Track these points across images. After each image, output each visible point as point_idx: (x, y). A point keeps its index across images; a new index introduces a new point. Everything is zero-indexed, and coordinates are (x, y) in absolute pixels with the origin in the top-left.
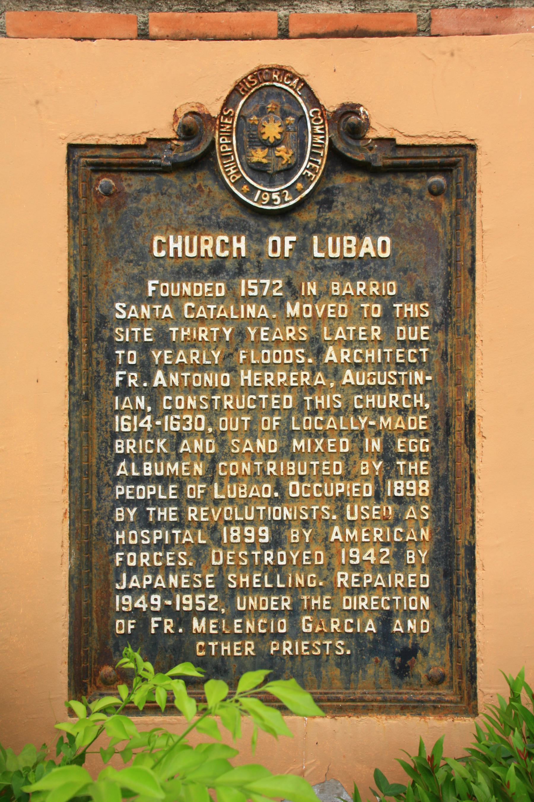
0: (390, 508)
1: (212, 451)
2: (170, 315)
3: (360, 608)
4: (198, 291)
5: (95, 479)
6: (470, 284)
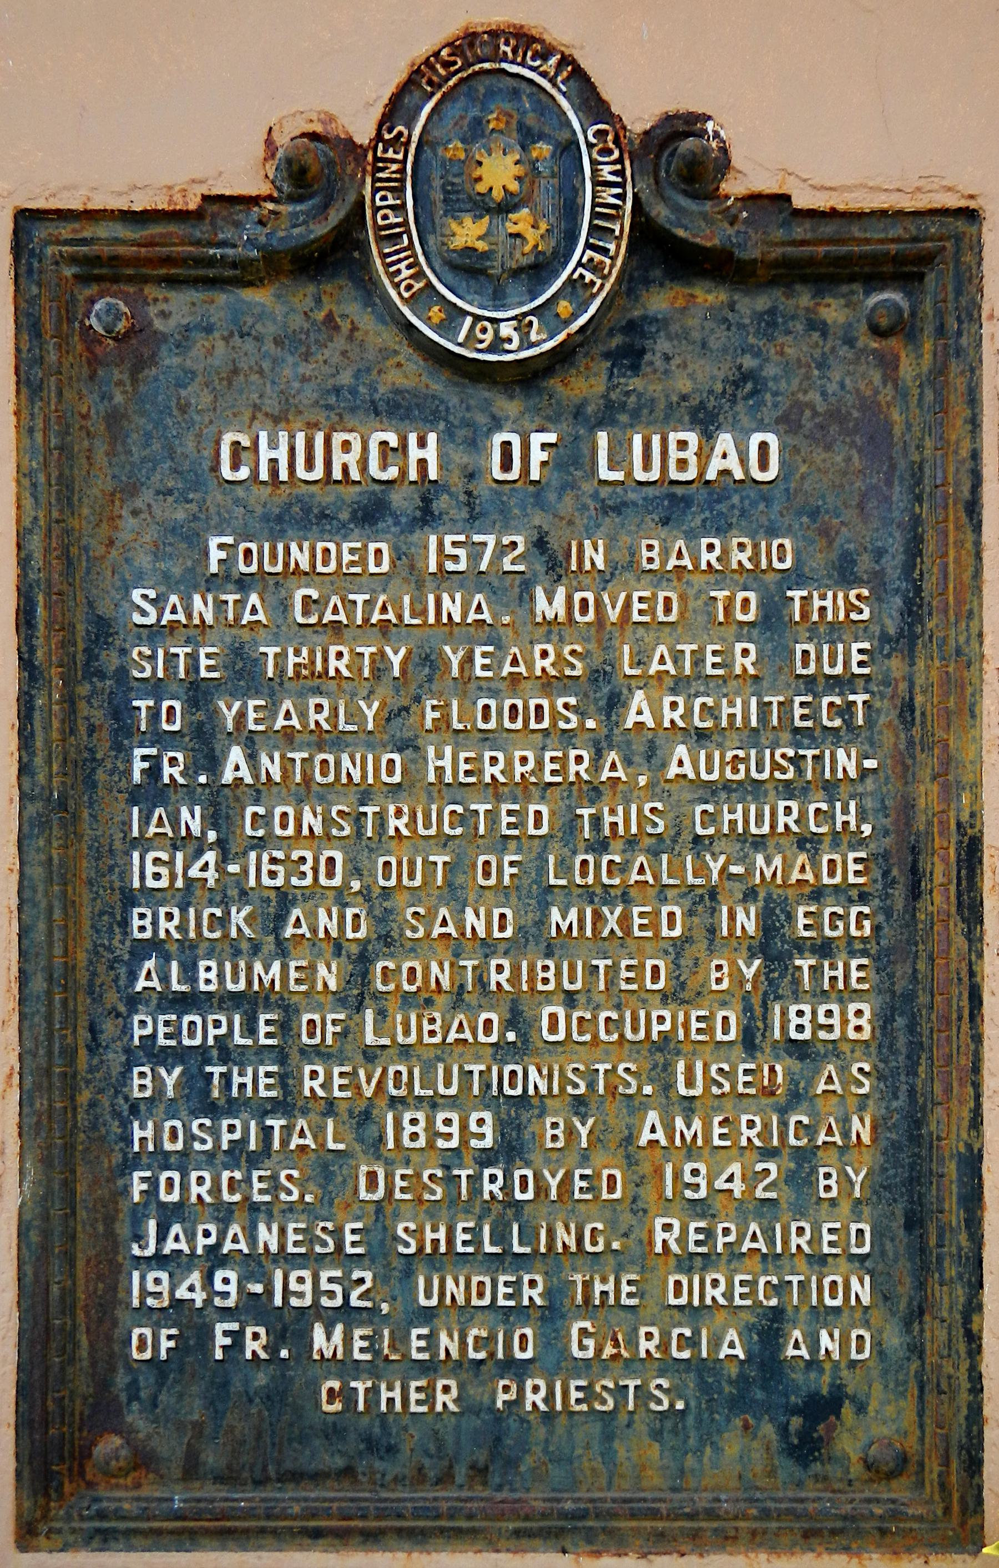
0: (778, 1068)
2: (261, 616)
3: (708, 1301)
4: (326, 563)
5: (83, 1002)
6: (970, 537)
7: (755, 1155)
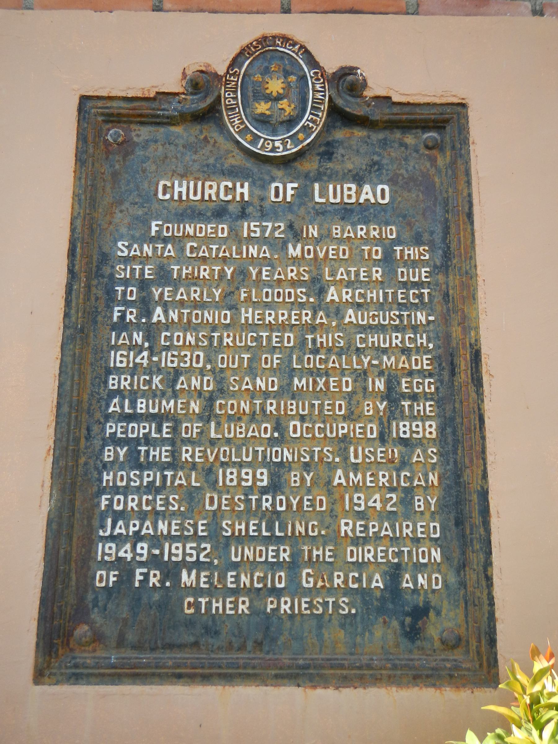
0: (395, 450)
1: (210, 388)
2: (172, 254)
3: (366, 560)
4: (200, 232)
5: (85, 416)
6: (469, 227)
7: (386, 490)
